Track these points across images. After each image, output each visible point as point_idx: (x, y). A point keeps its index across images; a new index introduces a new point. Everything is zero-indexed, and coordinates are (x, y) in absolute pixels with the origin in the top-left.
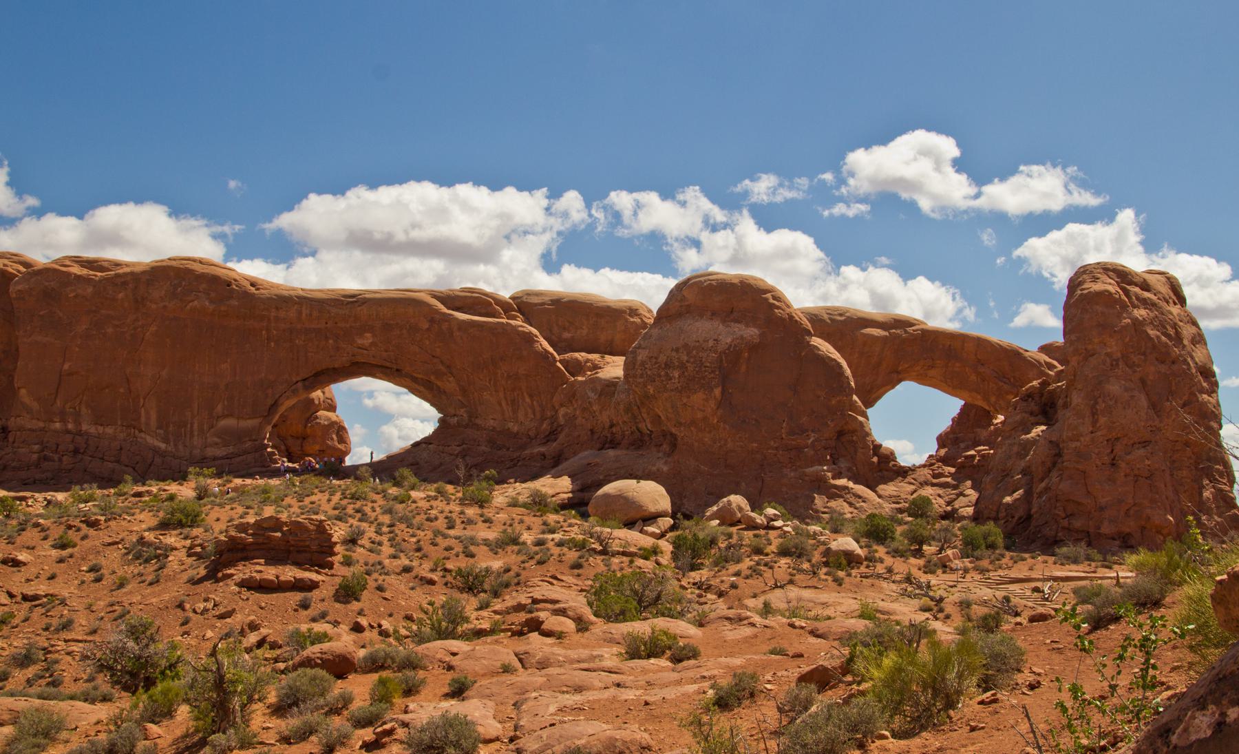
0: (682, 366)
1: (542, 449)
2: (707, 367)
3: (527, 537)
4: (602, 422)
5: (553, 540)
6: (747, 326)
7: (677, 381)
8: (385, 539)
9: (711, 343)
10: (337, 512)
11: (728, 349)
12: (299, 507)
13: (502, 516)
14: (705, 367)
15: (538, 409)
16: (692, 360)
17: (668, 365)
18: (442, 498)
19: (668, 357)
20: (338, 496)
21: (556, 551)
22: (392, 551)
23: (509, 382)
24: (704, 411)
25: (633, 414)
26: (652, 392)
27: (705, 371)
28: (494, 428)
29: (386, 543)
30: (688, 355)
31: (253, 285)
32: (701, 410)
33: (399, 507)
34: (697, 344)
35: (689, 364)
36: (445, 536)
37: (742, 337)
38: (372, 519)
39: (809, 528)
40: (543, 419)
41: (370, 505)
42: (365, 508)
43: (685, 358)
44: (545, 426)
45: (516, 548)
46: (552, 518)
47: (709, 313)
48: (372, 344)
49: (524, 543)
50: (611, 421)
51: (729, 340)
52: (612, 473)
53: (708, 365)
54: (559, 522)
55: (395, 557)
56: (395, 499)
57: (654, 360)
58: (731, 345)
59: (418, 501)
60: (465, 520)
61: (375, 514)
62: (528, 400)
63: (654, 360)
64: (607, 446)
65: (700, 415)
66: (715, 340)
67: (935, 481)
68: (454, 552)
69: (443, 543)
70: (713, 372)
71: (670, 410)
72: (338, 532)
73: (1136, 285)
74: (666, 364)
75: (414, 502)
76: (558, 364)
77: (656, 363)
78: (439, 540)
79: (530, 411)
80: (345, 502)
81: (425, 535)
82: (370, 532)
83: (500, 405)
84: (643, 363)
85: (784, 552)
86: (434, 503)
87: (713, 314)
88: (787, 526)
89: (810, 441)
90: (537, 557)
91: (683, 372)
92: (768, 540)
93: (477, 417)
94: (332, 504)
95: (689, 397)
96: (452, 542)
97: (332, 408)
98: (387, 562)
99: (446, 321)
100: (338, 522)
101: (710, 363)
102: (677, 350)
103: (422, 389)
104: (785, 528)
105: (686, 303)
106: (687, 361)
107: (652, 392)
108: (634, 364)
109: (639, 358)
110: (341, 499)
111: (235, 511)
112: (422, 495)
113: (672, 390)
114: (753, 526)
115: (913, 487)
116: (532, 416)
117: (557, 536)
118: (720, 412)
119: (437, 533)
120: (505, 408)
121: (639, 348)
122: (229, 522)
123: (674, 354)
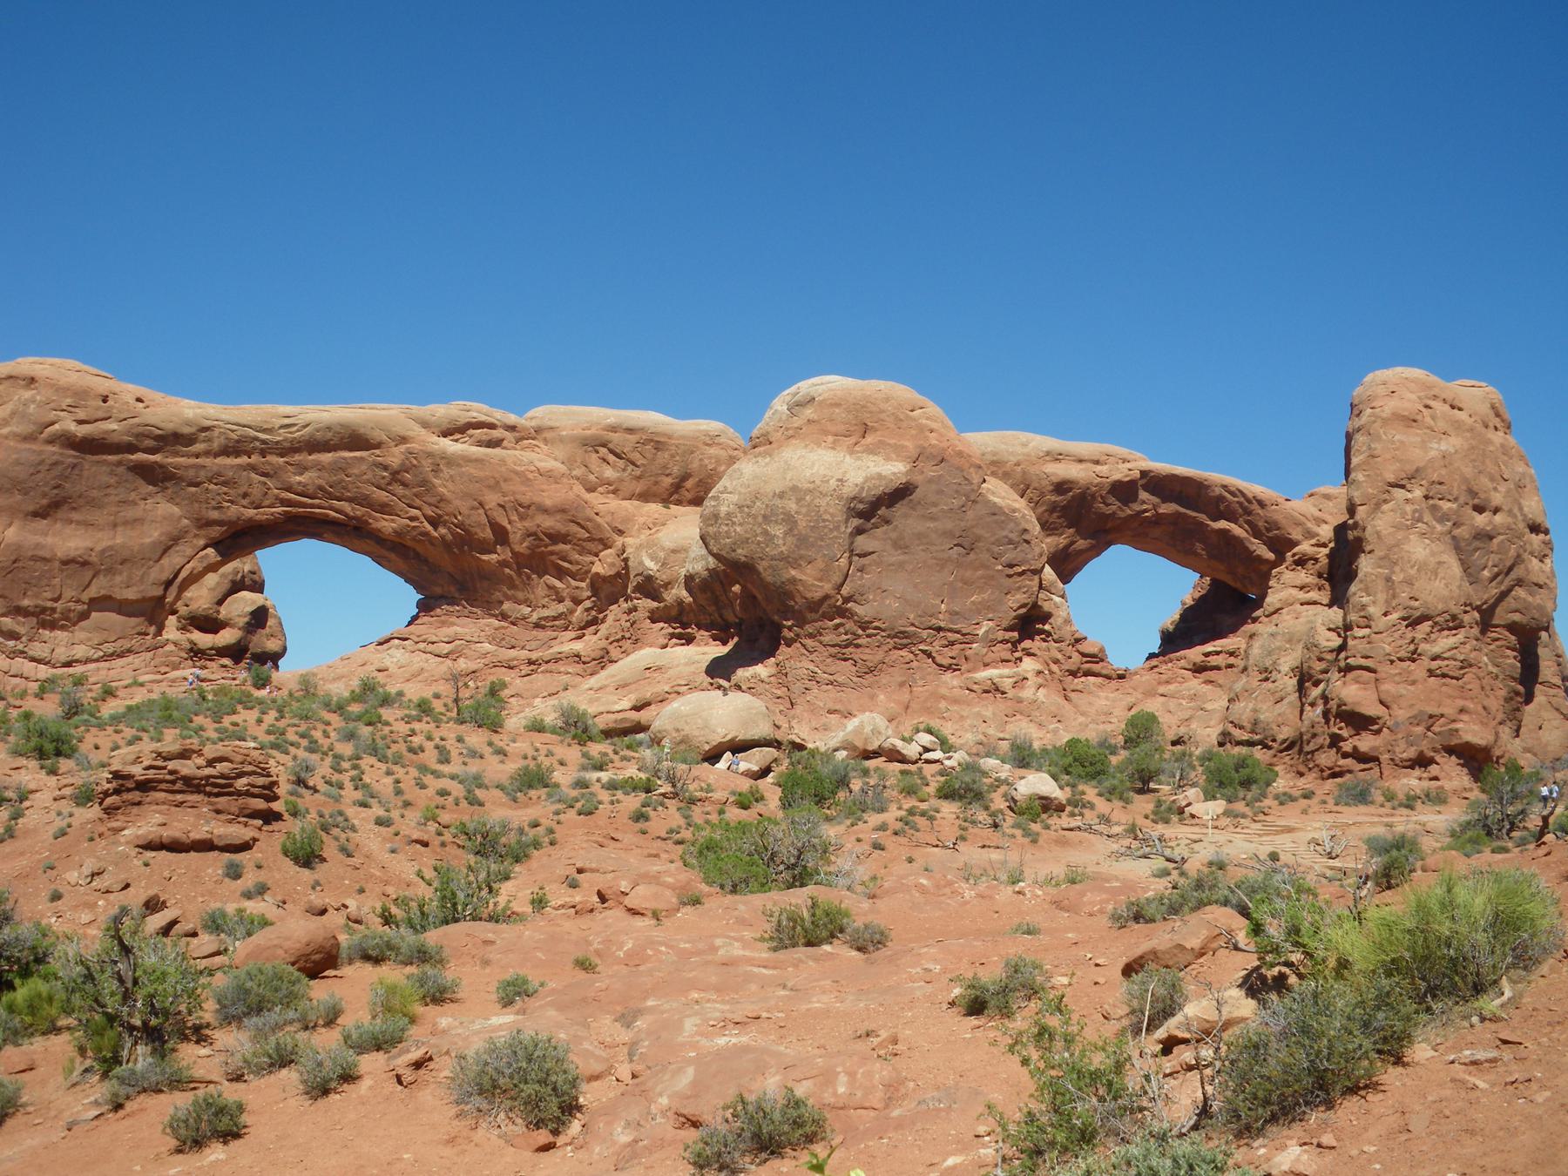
3: (562, 777)
5: (598, 780)
6: (888, 459)
7: (781, 542)
8: (345, 778)
9: (833, 483)
10: (272, 738)
12: (216, 730)
13: (522, 746)
14: (824, 521)
16: (804, 510)
18: (428, 719)
20: (273, 714)
21: (605, 796)
22: (358, 795)
29: (349, 785)
31: (139, 400)
33: (365, 731)
34: (811, 486)
36: (437, 774)
37: (880, 476)
38: (325, 749)
39: (982, 761)
41: (321, 727)
42: (313, 733)
45: (543, 792)
46: (596, 749)
49: (557, 785)
51: (860, 480)
54: (606, 754)
55: (364, 805)
56: (358, 718)
58: (863, 488)
59: (394, 723)
60: (465, 751)
61: (329, 741)
66: (838, 480)
67: (1162, 689)
68: (450, 799)
69: (434, 784)
72: (281, 768)
73: (1445, 401)
74: (765, 517)
75: (387, 724)
76: (598, 519)
78: (428, 779)
80: (282, 724)
81: (408, 776)
82: (324, 768)
84: (728, 514)
85: (947, 794)
86: (417, 726)
88: (949, 758)
89: (981, 632)
90: (578, 805)
92: (923, 778)
94: (264, 726)
96: (445, 783)
97: (258, 587)
98: (351, 812)
100: (274, 753)
102: (782, 495)
103: (393, 556)
104: (947, 763)
110: (277, 719)
111: (122, 735)
112: (400, 713)
114: (895, 756)
115: (1131, 700)
117: (605, 776)
119: (423, 769)
122: (113, 750)
123: (778, 502)
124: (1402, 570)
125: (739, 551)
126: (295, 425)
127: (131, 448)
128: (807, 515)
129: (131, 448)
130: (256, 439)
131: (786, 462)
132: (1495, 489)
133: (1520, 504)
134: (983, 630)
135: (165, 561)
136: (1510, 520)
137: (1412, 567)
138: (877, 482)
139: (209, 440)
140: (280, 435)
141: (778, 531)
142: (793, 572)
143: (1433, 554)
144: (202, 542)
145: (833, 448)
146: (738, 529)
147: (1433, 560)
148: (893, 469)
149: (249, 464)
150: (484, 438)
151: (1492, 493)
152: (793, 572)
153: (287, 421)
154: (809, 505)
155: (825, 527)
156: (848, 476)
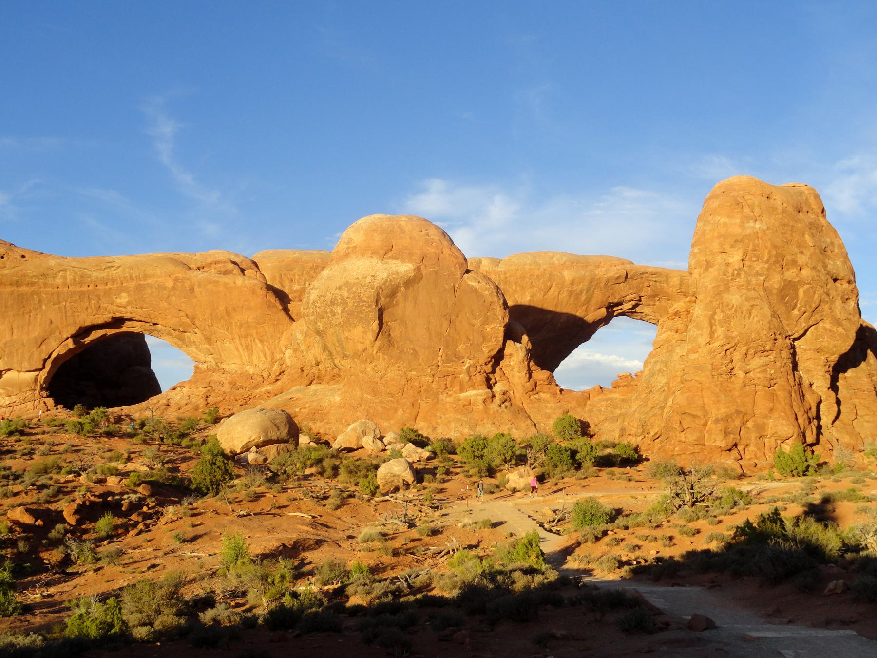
0: (344, 303)
1: (269, 388)
2: (365, 301)
4: (309, 361)
9: (369, 279)
11: (385, 283)
14: (363, 302)
15: (268, 353)
16: (352, 296)
17: (333, 303)
19: (333, 295)
23: (242, 330)
24: (363, 343)
25: (329, 351)
26: (321, 328)
27: (363, 306)
28: (236, 371)
30: (348, 292)
32: (361, 342)
34: (357, 281)
35: (349, 300)
40: (273, 361)
43: (346, 294)
44: (275, 367)
47: (370, 252)
48: (129, 303)
50: (316, 359)
51: (385, 276)
52: (308, 406)
53: (366, 299)
57: (323, 299)
58: (387, 280)
62: (259, 345)
63: (323, 299)
64: (314, 381)
65: (360, 347)
66: (372, 276)
70: (370, 306)
71: (337, 345)
74: (331, 302)
77: (324, 301)
79: (262, 355)
83: (237, 349)
84: (314, 302)
87: (373, 253)
91: (344, 308)
93: (222, 362)
95: (350, 331)
99: (188, 279)
101: (367, 298)
102: (340, 288)
105: (354, 245)
106: (348, 298)
107: (321, 328)
108: (308, 303)
109: (312, 298)
113: (336, 325)
116: (265, 360)
118: (378, 343)
120: (242, 353)
121: (312, 289)
123: (337, 291)
124: (722, 311)
125: (319, 324)
126: (113, 266)
127: (17, 284)
128: (353, 298)
129: (17, 284)
130: (90, 276)
131: (345, 267)
132: (802, 253)
133: (824, 263)
134: (467, 365)
135: (43, 347)
136: (814, 273)
137: (730, 309)
138: (396, 276)
139: (65, 278)
140: (104, 273)
141: (339, 310)
142: (347, 334)
143: (747, 299)
144: (65, 337)
145: (372, 257)
146: (318, 310)
147: (747, 305)
148: (405, 268)
149: (88, 290)
150: (222, 269)
151: (799, 255)
152: (347, 334)
153: (109, 265)
154: (354, 293)
155: (363, 306)
156: (378, 273)
